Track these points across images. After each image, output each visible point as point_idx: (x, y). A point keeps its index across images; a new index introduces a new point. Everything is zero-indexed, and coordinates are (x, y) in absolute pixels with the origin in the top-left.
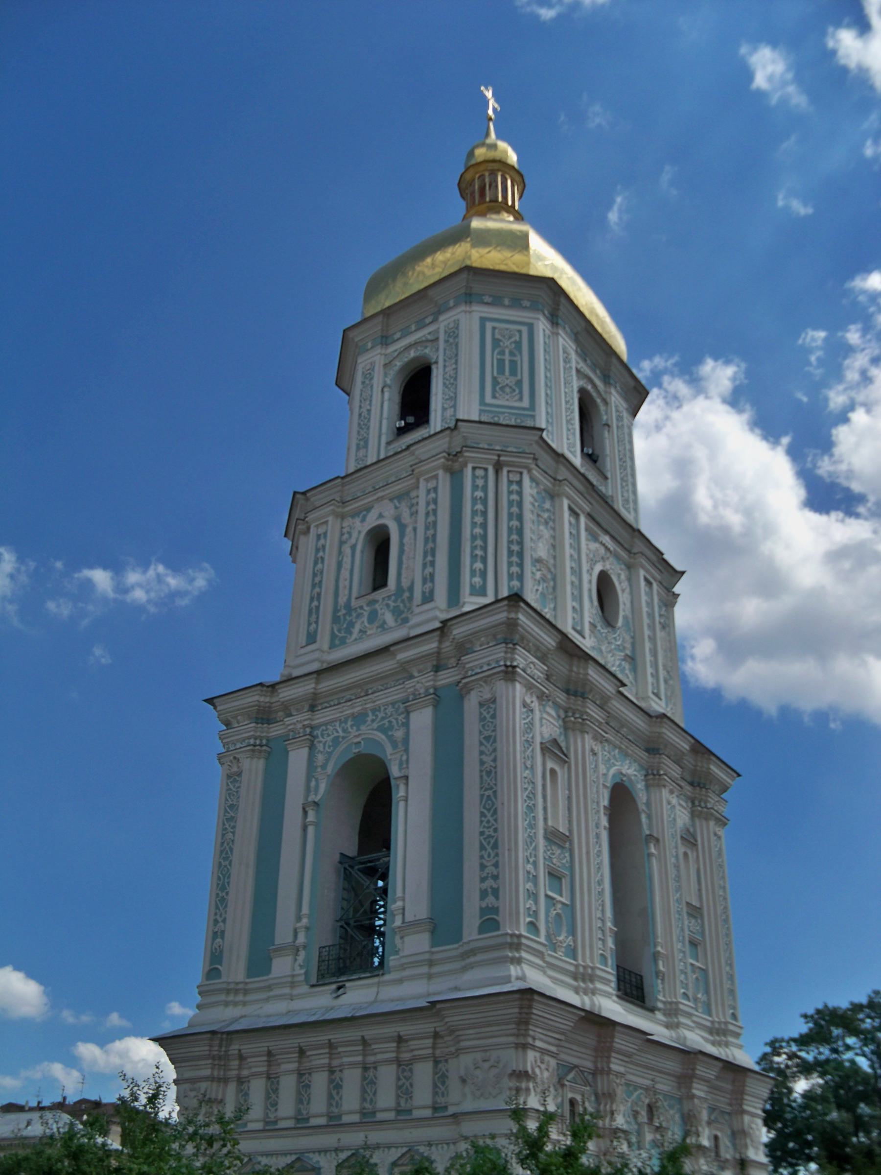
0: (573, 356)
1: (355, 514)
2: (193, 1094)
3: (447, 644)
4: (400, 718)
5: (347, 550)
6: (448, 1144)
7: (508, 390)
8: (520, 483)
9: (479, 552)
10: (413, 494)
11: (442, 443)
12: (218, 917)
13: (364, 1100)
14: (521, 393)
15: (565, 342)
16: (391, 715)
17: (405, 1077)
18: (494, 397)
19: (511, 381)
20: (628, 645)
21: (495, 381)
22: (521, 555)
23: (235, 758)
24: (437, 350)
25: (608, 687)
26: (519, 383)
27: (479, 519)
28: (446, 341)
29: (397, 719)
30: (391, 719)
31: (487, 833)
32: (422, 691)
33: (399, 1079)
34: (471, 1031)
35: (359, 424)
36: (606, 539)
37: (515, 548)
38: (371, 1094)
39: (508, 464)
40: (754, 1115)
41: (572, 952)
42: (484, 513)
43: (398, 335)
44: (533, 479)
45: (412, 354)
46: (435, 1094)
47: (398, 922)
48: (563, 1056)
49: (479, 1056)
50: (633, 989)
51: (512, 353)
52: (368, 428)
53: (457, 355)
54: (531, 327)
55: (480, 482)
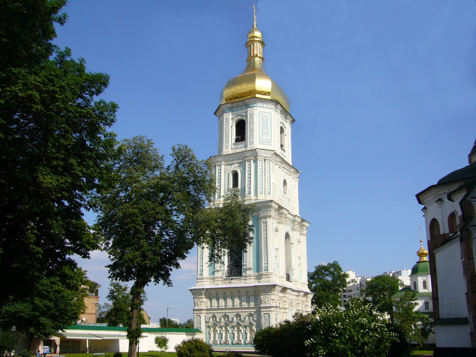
0: (280, 118)
1: (228, 165)
5: (227, 175)
10: (244, 163)
14: (268, 135)
20: (288, 197)
25: (286, 212)
26: (268, 131)
39: (267, 160)
40: (309, 302)
41: (279, 273)
43: (235, 109)
44: (272, 162)
47: (245, 267)
48: (279, 295)
50: (288, 278)
51: (266, 123)
52: (228, 137)
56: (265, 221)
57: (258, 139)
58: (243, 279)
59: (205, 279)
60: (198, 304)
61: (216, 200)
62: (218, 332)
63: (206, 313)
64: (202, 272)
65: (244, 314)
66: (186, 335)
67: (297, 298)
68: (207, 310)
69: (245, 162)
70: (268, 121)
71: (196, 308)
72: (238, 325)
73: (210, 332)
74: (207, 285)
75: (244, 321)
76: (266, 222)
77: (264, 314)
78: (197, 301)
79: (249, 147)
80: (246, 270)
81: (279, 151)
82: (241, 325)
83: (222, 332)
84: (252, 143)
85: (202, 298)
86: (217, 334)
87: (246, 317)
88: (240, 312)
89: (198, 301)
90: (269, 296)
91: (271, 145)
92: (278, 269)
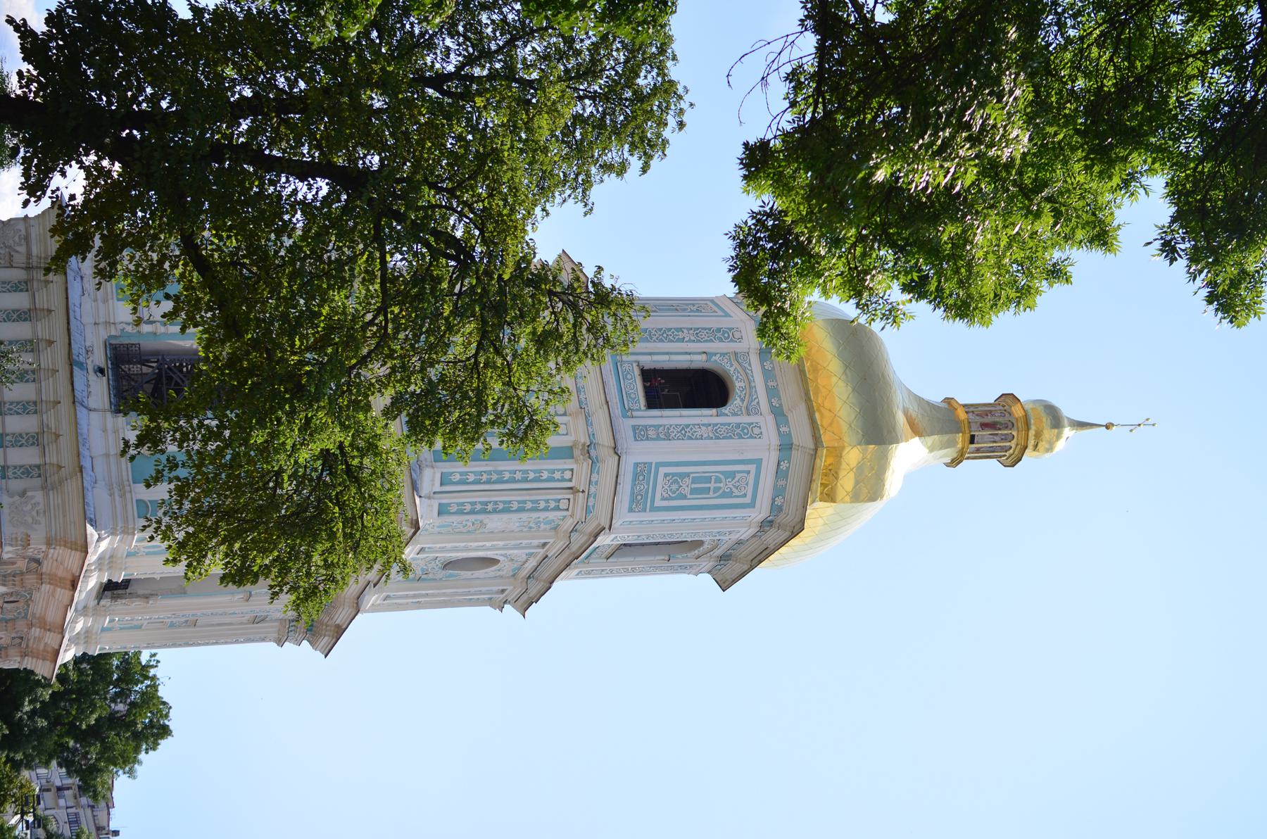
2: (17, 238)
7: (674, 487)
8: (557, 508)
9: (485, 477)
11: (604, 438)
13: (11, 403)
15: (745, 533)
18: (666, 475)
19: (687, 491)
20: (431, 576)
21: (688, 475)
22: (484, 511)
24: (735, 414)
26: (684, 497)
27: (518, 476)
28: (738, 425)
35: (669, 330)
36: (532, 563)
37: (490, 507)
42: (525, 480)
45: (738, 384)
49: (41, 507)
50: (111, 589)
52: (661, 341)
53: (718, 438)
54: (752, 505)
55: (557, 475)
57: (654, 459)
69: (565, 414)
70: (724, 495)
79: (625, 426)
81: (605, 540)
84: (640, 433)
91: (631, 510)
92: (148, 554)
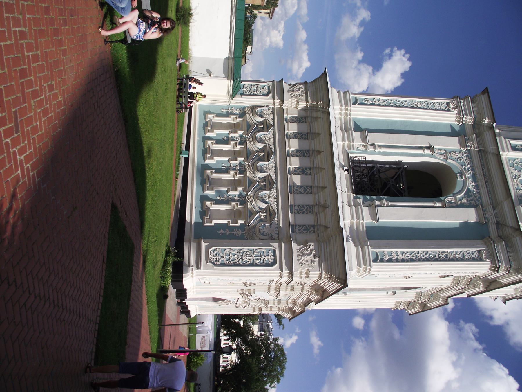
3: (510, 231)
4: (473, 202)
6: (278, 234)
12: (381, 101)
16: (475, 197)
17: (307, 209)
23: (457, 107)
29: (472, 200)
30: (473, 196)
31: (418, 255)
32: (487, 216)
33: (307, 206)
34: (328, 250)
38: (300, 190)
46: (300, 226)
47: (377, 203)
56: (484, 255)
58: (349, 196)
59: (346, 109)
60: (293, 91)
61: (507, 140)
62: (232, 135)
63: (273, 109)
64: (359, 104)
65: (271, 197)
66: (229, 58)
67: (290, 301)
68: (281, 111)
71: (286, 87)
72: (249, 183)
73: (233, 117)
74: (336, 112)
75: (256, 197)
76: (481, 260)
77: (274, 252)
78: (299, 90)
80: (369, 206)
82: (246, 190)
83: (232, 143)
85: (307, 101)
86: (227, 132)
87: (266, 202)
88: (277, 190)
89: (300, 92)
90: (316, 264)
